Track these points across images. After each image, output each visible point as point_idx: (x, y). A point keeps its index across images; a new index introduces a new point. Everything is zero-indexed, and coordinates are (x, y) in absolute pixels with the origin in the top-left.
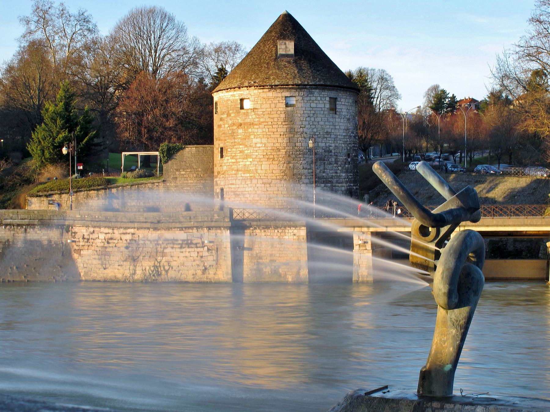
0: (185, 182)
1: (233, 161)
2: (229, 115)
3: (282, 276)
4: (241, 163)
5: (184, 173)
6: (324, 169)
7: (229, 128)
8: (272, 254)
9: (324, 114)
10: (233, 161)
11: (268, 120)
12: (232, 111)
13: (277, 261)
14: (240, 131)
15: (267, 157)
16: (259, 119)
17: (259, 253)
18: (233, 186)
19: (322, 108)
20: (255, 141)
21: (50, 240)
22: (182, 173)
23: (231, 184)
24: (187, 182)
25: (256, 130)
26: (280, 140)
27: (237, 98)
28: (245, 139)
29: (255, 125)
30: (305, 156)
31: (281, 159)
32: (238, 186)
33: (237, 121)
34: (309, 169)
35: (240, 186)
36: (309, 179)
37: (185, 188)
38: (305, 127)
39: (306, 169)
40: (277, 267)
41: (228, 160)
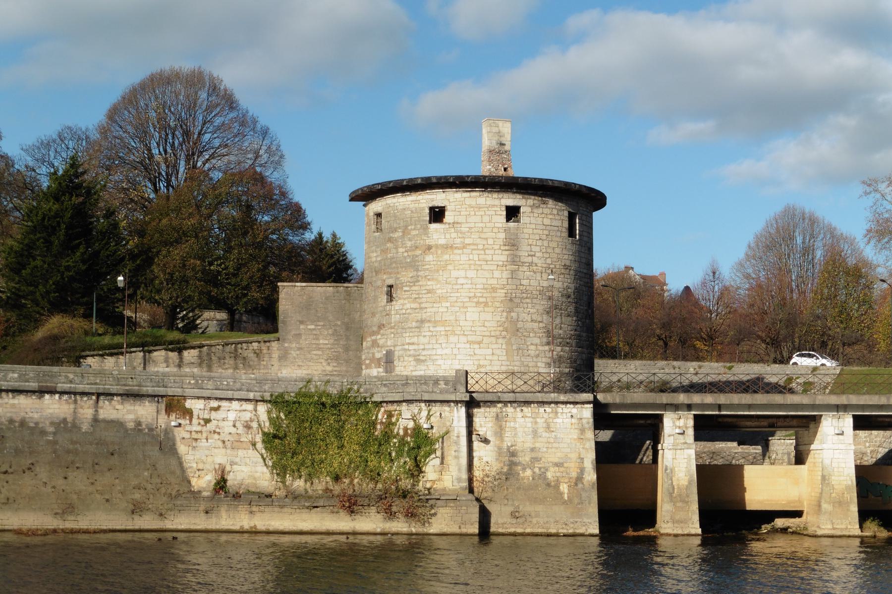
0: (314, 342)
3: (553, 484)
5: (313, 327)
6: (561, 323)
7: (406, 254)
8: (535, 448)
9: (561, 236)
11: (478, 241)
12: (413, 227)
13: (543, 460)
14: (429, 258)
15: (475, 300)
16: (462, 240)
17: (512, 446)
18: (411, 347)
19: (558, 227)
20: (455, 274)
21: (139, 422)
22: (309, 327)
23: (409, 344)
24: (317, 342)
25: (458, 258)
26: (497, 274)
27: (424, 205)
28: (438, 271)
29: (456, 248)
30: (535, 301)
31: (498, 304)
32: (422, 347)
33: (422, 242)
34: (540, 322)
35: (427, 347)
36: (539, 337)
37: (315, 352)
38: (534, 256)
39: (536, 322)
40: (542, 470)
41: (403, 305)
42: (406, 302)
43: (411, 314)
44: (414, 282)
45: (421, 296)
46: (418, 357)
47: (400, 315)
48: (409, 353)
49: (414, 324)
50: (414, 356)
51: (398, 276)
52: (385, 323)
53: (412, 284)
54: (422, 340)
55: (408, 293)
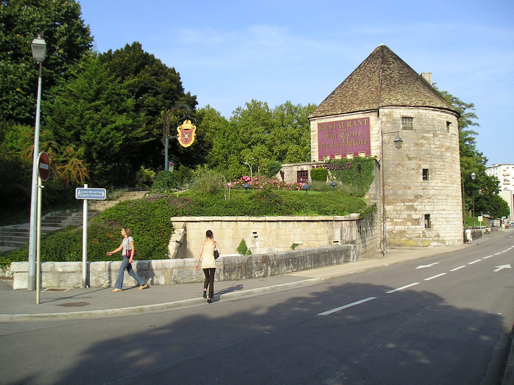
2: (435, 135)
7: (436, 149)
10: (443, 185)
12: (440, 132)
14: (448, 154)
18: (443, 212)
27: (444, 119)
41: (437, 183)
42: (438, 181)
43: (442, 190)
45: (446, 179)
47: (435, 190)
48: (442, 216)
51: (432, 163)
52: (422, 194)
53: (441, 170)
54: (449, 208)
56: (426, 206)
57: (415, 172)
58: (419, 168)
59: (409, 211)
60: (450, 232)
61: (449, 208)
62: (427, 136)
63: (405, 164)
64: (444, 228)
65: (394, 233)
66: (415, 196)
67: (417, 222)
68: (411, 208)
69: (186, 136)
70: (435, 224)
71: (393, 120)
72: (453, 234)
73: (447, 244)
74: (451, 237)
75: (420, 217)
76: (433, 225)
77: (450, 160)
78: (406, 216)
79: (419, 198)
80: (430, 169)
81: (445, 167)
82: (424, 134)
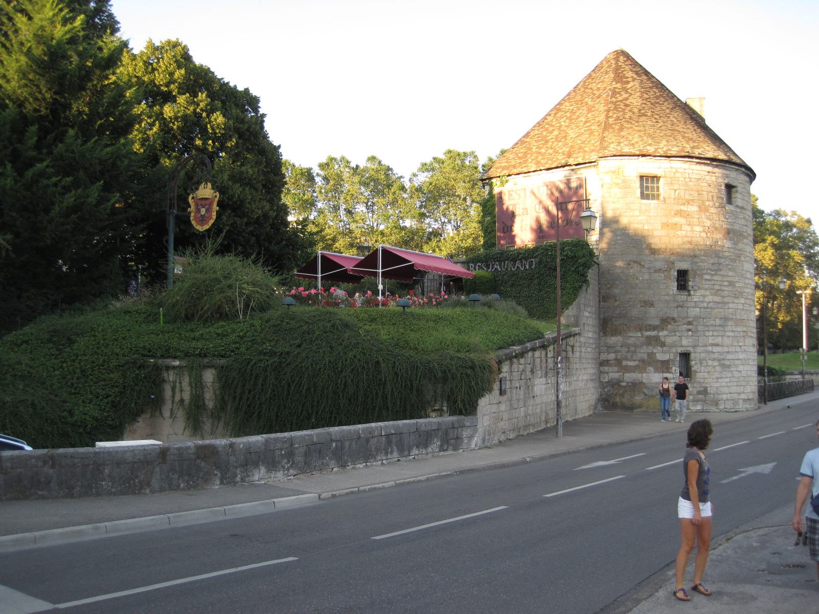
1: (717, 299)
4: (731, 305)
10: (717, 299)
18: (715, 349)
23: (713, 345)
32: (726, 349)
35: (731, 350)
41: (704, 296)
42: (708, 293)
43: (714, 308)
44: (716, 270)
45: (723, 288)
46: (723, 362)
47: (700, 308)
48: (712, 356)
49: (718, 322)
50: (719, 360)
51: (696, 260)
52: (676, 316)
53: (713, 273)
54: (727, 341)
55: (710, 283)
56: (683, 338)
57: (663, 275)
58: (670, 269)
59: (651, 348)
60: (729, 384)
61: (727, 341)
62: (686, 209)
63: (645, 261)
64: (717, 378)
65: (623, 386)
66: (662, 320)
67: (665, 366)
68: (657, 341)
69: (203, 211)
70: (699, 370)
71: (624, 181)
72: (734, 389)
73: (722, 407)
74: (729, 395)
75: (672, 358)
76: (696, 372)
77: (731, 254)
78: (645, 356)
79: (669, 323)
80: (692, 269)
81: (721, 267)
82: (683, 208)
